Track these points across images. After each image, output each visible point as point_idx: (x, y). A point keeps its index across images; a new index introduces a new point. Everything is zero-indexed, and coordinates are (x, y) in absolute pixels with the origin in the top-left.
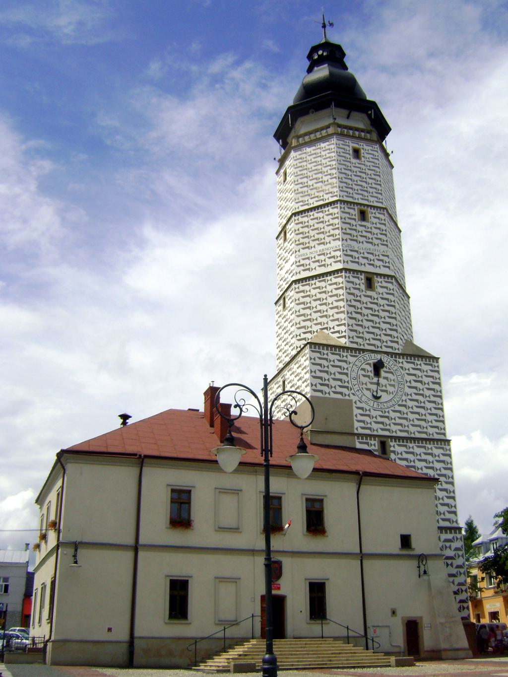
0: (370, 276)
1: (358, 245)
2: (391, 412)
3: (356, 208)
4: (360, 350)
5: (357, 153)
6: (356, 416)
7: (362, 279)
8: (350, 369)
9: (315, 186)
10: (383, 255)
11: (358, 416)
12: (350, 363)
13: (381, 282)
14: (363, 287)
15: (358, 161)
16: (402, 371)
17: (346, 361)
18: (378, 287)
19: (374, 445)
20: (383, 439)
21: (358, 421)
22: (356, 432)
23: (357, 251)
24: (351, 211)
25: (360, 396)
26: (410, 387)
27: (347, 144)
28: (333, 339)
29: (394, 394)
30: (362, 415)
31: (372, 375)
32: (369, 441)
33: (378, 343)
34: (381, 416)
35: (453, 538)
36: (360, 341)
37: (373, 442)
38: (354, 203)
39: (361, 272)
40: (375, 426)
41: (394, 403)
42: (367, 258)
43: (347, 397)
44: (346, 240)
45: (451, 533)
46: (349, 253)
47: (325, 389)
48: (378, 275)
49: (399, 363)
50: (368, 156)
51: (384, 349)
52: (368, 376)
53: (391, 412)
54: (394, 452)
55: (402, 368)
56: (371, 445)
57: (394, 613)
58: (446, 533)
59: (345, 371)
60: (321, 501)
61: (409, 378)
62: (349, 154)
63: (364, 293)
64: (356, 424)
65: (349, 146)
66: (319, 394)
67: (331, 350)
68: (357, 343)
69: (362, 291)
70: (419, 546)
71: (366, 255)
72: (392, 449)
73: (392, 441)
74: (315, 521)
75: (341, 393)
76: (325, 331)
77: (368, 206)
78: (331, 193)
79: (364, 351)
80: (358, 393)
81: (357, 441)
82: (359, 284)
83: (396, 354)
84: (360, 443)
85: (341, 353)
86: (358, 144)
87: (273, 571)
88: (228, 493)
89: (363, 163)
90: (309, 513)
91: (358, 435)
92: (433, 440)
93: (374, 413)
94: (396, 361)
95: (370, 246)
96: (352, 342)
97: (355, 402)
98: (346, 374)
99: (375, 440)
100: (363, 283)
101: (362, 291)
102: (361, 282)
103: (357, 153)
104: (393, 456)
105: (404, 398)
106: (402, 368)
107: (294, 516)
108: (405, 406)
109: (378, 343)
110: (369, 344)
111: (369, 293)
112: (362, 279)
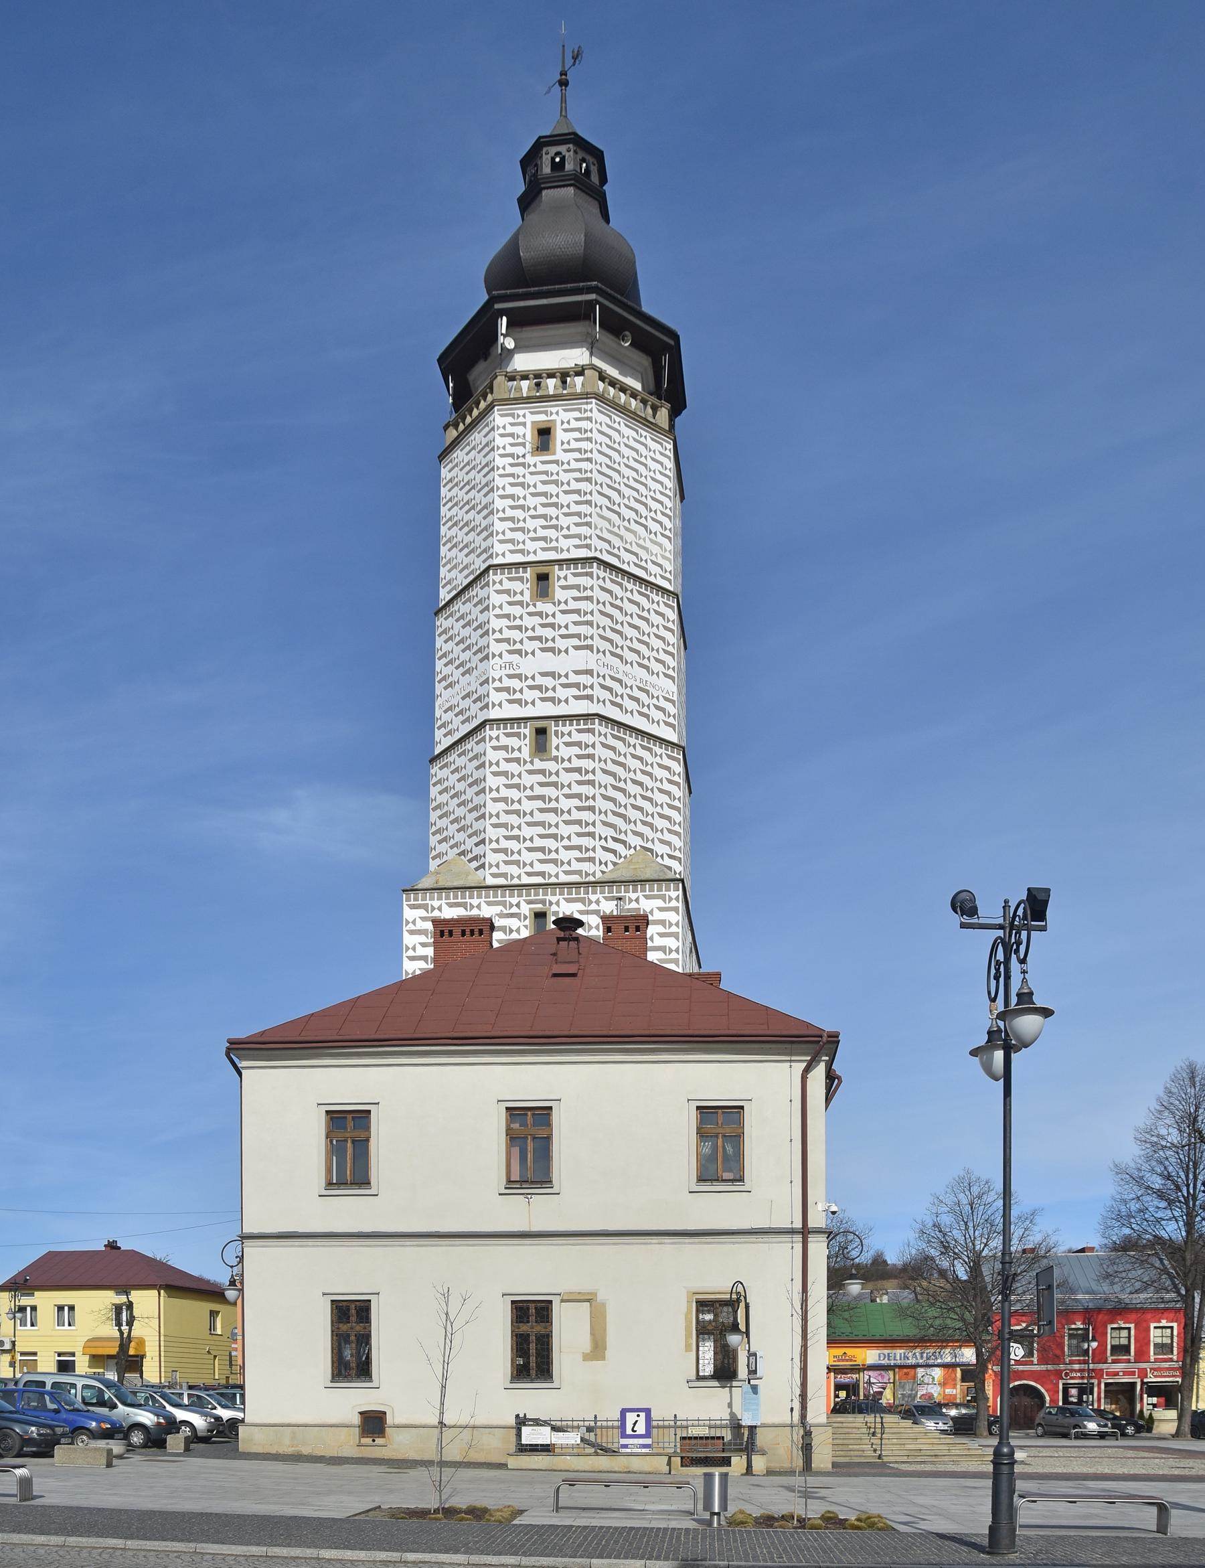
14: (525, 754)
27: (521, 419)
62: (524, 445)
63: (529, 766)
65: (524, 424)
67: (447, 898)
68: (505, 875)
69: (525, 762)
86: (546, 413)
101: (525, 762)
103: (544, 434)
110: (529, 874)
112: (525, 736)
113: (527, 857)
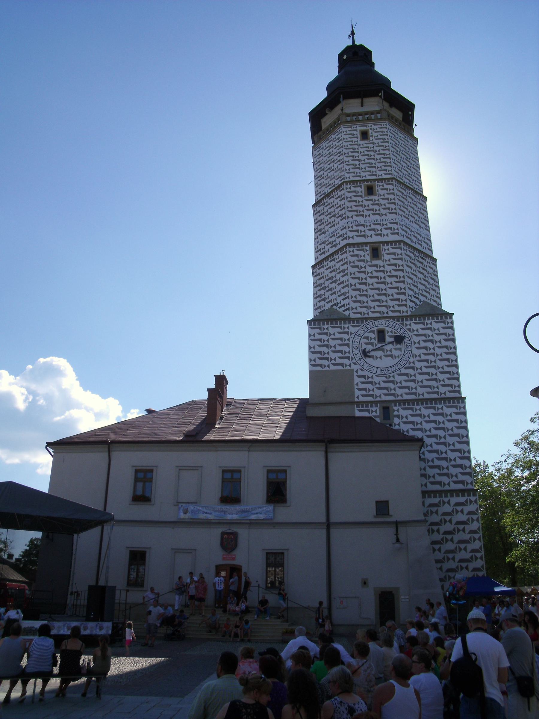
0: (375, 246)
1: (364, 219)
2: (396, 376)
3: (363, 185)
4: (362, 320)
5: (365, 135)
6: (357, 384)
7: (367, 251)
8: (351, 340)
9: (329, 175)
10: (391, 223)
11: (360, 384)
12: (351, 334)
13: (388, 249)
14: (368, 258)
15: (366, 142)
16: (409, 332)
17: (347, 333)
18: (385, 255)
19: (376, 412)
20: (385, 405)
21: (359, 389)
22: (356, 400)
23: (363, 225)
24: (358, 189)
25: (362, 364)
26: (418, 348)
27: (355, 129)
28: (339, 313)
29: (400, 358)
30: (363, 383)
31: (375, 342)
32: (369, 408)
33: (384, 309)
34: (385, 382)
35: (466, 501)
36: (364, 310)
37: (374, 409)
38: (360, 181)
39: (366, 244)
40: (377, 392)
41: (399, 366)
42: (374, 230)
43: (348, 368)
44: (352, 217)
45: (463, 495)
46: (355, 228)
47: (325, 362)
48: (383, 243)
49: (406, 325)
50: (376, 134)
51: (391, 314)
52: (372, 344)
53: (396, 376)
54: (398, 416)
55: (410, 330)
56: (372, 411)
57: (365, 583)
58: (458, 496)
59: (347, 342)
60: (285, 471)
61: (416, 339)
62: (357, 138)
63: (369, 263)
64: (357, 393)
65: (356, 130)
66: (319, 368)
67: (332, 324)
68: (360, 313)
69: (367, 261)
70: (397, 512)
71: (373, 227)
72: (396, 413)
73: (395, 405)
74: (277, 492)
75: (342, 364)
76: (334, 307)
77: (375, 180)
78: (340, 177)
79: (366, 319)
80: (359, 362)
81: (356, 409)
82: (364, 256)
83: (402, 318)
84: (360, 411)
85: (343, 325)
87: (229, 542)
88: (189, 469)
89: (371, 142)
90: (270, 484)
91: (358, 403)
92: (445, 399)
93: (376, 379)
94: (403, 324)
95: (377, 217)
96: (355, 313)
97: (357, 372)
98: (348, 345)
99: (376, 406)
100: (368, 254)
101: (367, 261)
102: (366, 254)
103: (365, 135)
104: (396, 420)
105: (411, 360)
106: (410, 330)
107: (255, 488)
108: (413, 368)
109: (384, 309)
110: (373, 312)
111: (375, 262)
112: (367, 251)
113: (372, 304)
